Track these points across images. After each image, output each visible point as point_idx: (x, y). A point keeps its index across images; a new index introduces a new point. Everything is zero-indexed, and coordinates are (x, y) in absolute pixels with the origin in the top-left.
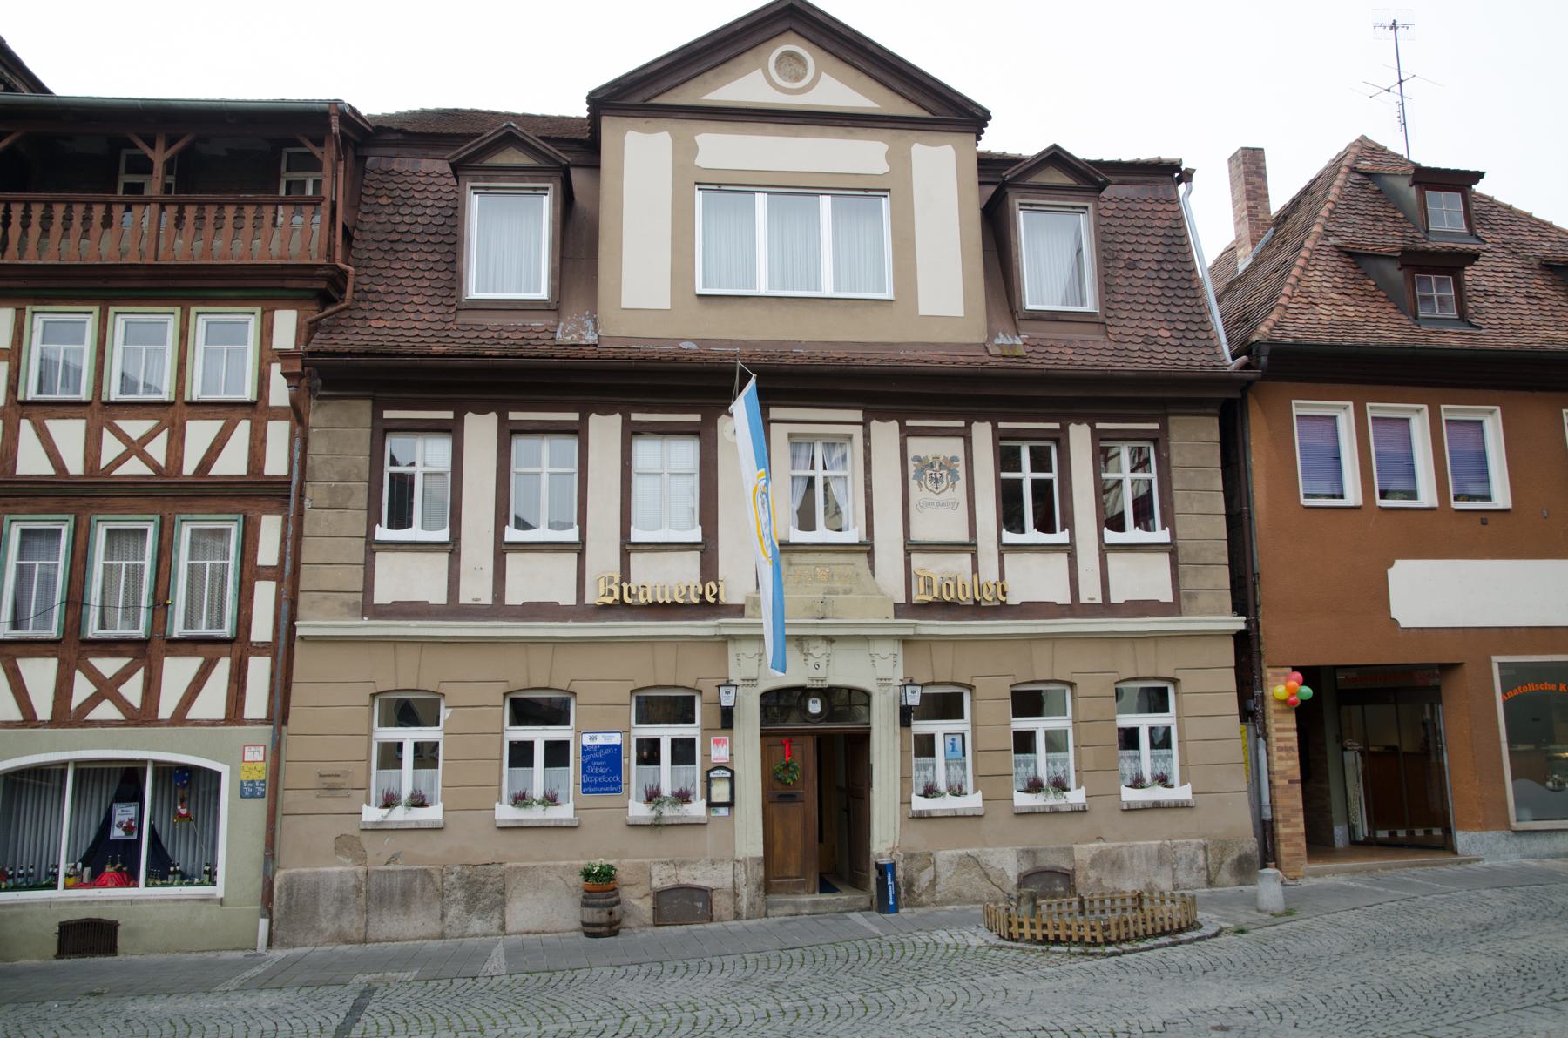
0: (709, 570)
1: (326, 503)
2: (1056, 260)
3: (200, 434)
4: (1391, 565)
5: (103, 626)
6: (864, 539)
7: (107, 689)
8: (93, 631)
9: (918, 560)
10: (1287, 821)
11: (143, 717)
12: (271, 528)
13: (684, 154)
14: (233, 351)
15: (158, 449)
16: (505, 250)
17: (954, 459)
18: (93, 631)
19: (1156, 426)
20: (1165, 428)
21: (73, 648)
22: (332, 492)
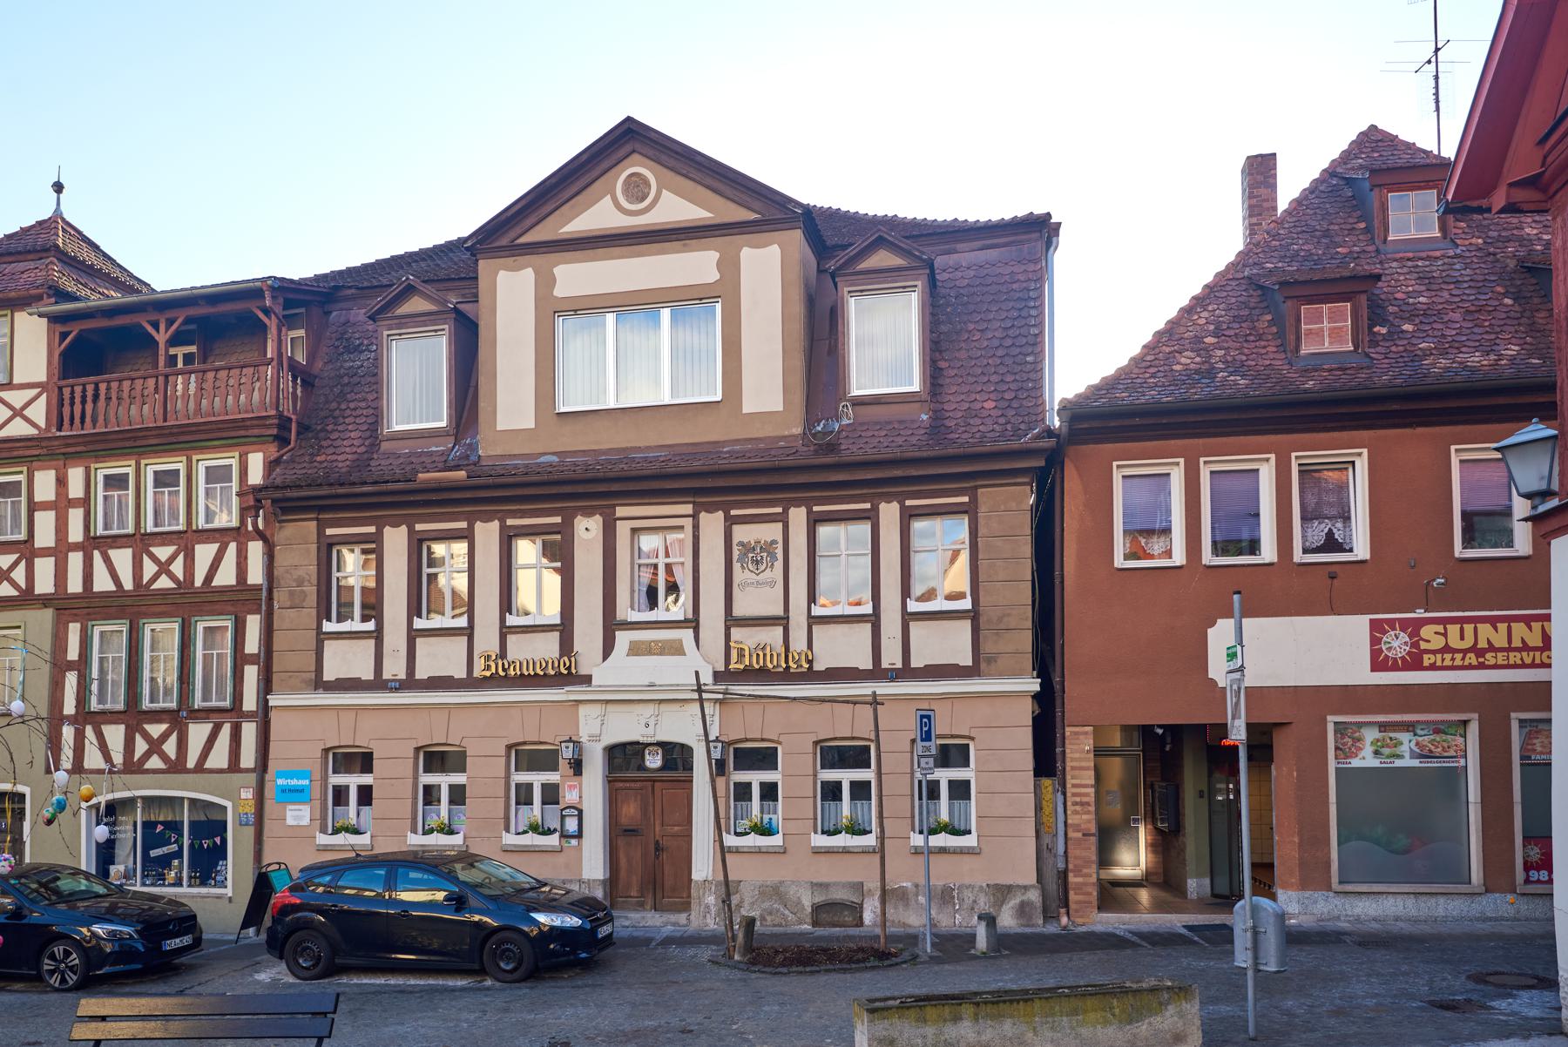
0: (566, 646)
1: (288, 604)
2: (886, 343)
3: (204, 553)
4: (1213, 624)
5: (152, 701)
6: (690, 616)
7: (155, 746)
8: (146, 704)
9: (736, 633)
10: (1078, 872)
11: (176, 766)
12: (253, 624)
13: (545, 283)
14: (218, 484)
15: (178, 568)
16: (413, 385)
17: (774, 542)
18: (146, 704)
19: (966, 499)
20: (974, 500)
21: (133, 717)
22: (292, 594)
